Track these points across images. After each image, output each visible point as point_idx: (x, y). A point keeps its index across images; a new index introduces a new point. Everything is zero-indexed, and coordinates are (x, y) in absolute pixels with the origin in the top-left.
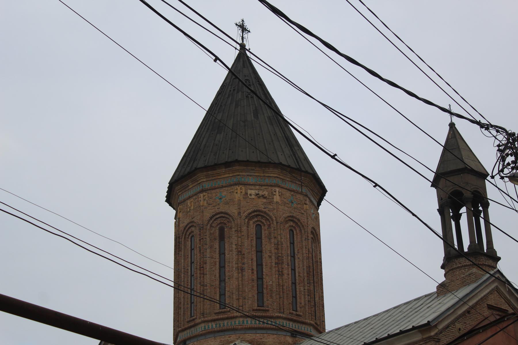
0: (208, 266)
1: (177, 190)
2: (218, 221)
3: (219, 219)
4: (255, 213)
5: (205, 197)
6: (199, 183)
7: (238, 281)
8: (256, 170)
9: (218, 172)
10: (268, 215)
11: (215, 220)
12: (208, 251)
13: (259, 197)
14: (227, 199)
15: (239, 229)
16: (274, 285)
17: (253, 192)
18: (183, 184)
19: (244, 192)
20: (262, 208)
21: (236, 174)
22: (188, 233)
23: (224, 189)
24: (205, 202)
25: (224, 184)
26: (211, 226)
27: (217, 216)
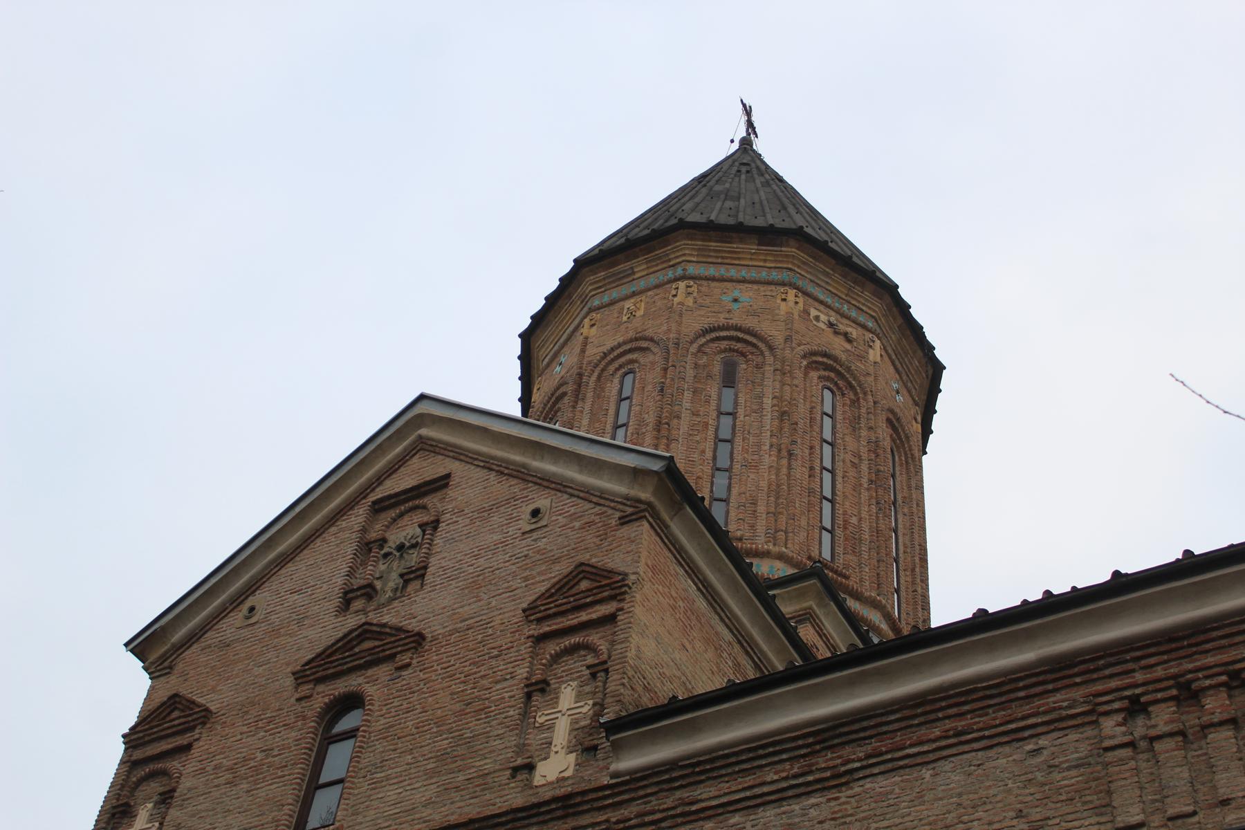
0: (684, 425)
1: (591, 284)
2: (724, 344)
3: (726, 342)
4: (825, 360)
5: (692, 289)
6: (673, 266)
7: (777, 475)
8: (833, 280)
9: (737, 248)
11: (713, 340)
16: (866, 527)
17: (823, 317)
18: (616, 268)
20: (843, 357)
21: (785, 266)
22: (616, 365)
23: (747, 285)
26: (700, 350)
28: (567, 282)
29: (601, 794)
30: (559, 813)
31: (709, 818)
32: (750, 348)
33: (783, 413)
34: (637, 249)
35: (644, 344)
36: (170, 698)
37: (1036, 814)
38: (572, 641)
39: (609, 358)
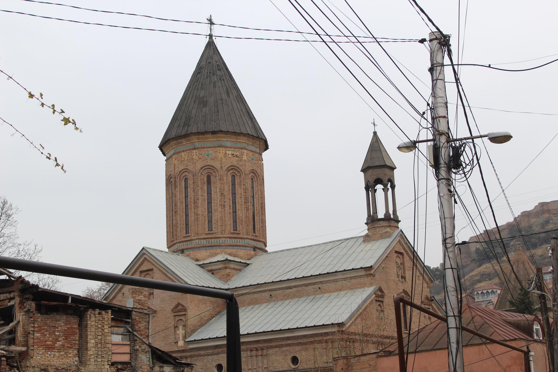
0: (200, 202)
2: (206, 171)
7: (222, 214)
10: (239, 169)
11: (204, 170)
12: (200, 191)
13: (234, 156)
14: (213, 156)
15: (222, 178)
17: (230, 152)
19: (224, 152)
21: (219, 139)
23: (211, 149)
24: (197, 157)
25: (211, 146)
26: (201, 174)
27: (206, 167)
33: (222, 194)
39: (181, 173)
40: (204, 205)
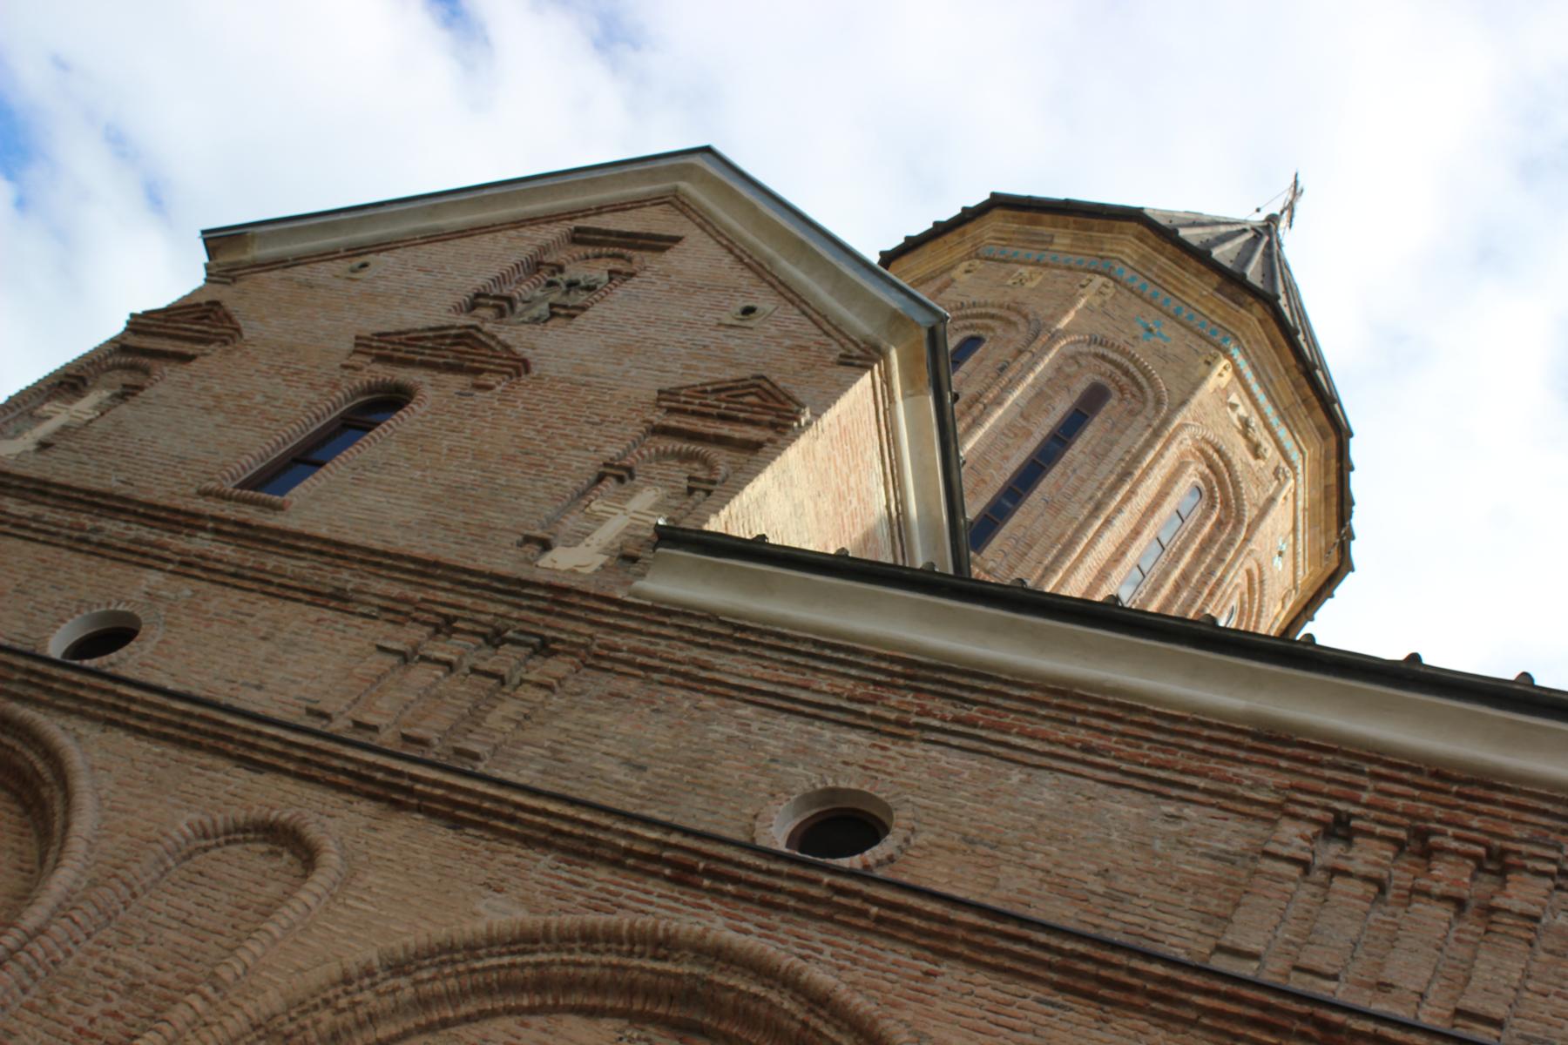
2: (1107, 367)
4: (1215, 456)
5: (1108, 291)
11: (1096, 355)
13: (1245, 435)
20: (1239, 467)
21: (1232, 330)
23: (1175, 324)
28: (969, 216)
29: (606, 607)
30: (542, 604)
31: (715, 694)
32: (1134, 389)
34: (1071, 219)
35: (1014, 317)
36: (209, 303)
37: (1123, 882)
38: (692, 447)
40: (1007, 446)
